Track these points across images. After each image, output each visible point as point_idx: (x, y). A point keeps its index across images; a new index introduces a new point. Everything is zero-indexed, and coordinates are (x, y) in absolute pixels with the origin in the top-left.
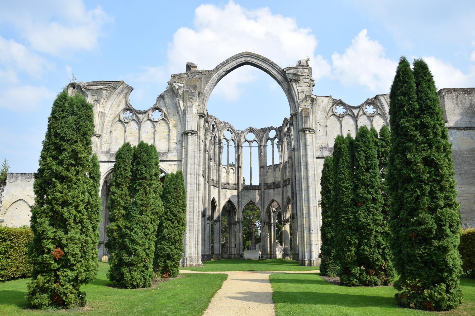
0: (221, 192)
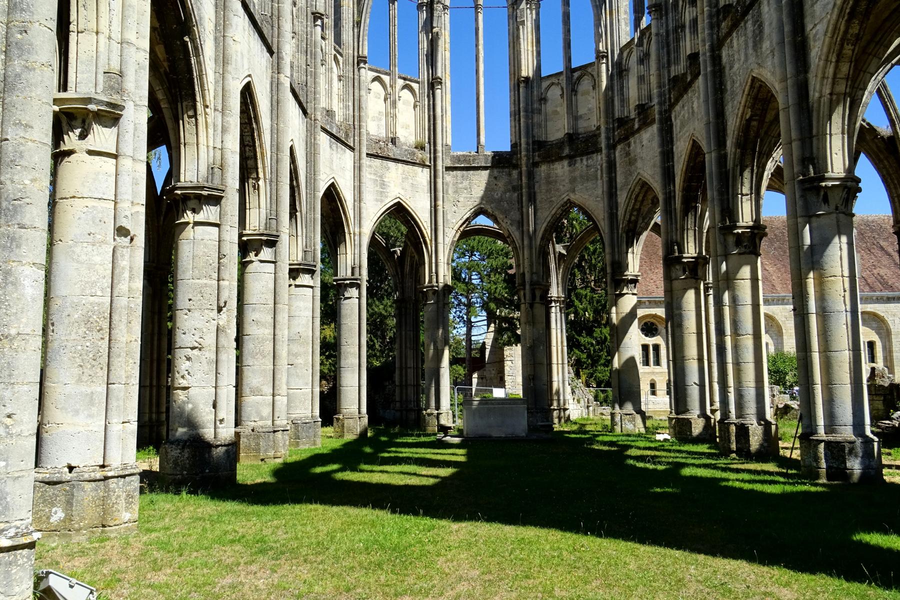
0: (364, 169)
